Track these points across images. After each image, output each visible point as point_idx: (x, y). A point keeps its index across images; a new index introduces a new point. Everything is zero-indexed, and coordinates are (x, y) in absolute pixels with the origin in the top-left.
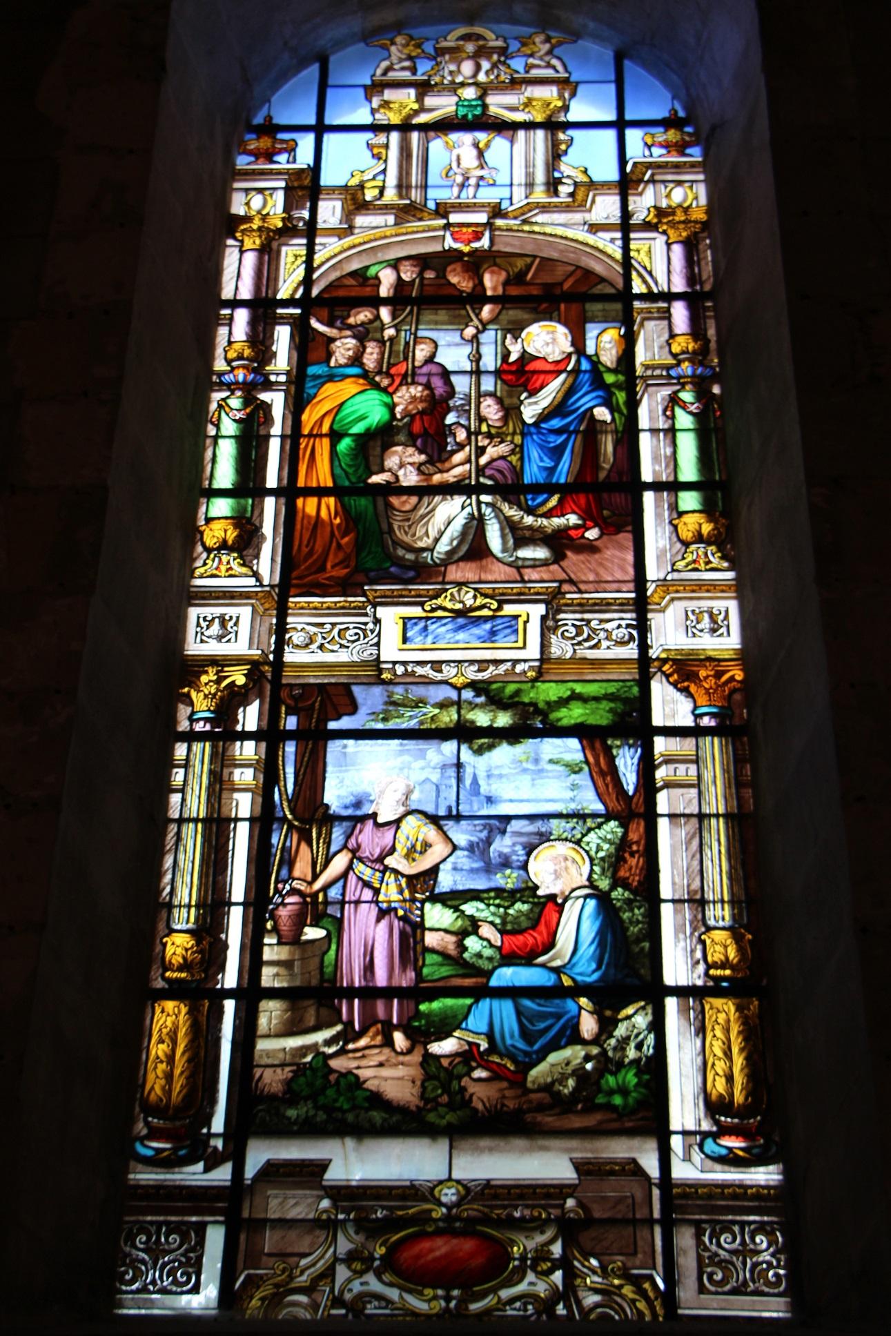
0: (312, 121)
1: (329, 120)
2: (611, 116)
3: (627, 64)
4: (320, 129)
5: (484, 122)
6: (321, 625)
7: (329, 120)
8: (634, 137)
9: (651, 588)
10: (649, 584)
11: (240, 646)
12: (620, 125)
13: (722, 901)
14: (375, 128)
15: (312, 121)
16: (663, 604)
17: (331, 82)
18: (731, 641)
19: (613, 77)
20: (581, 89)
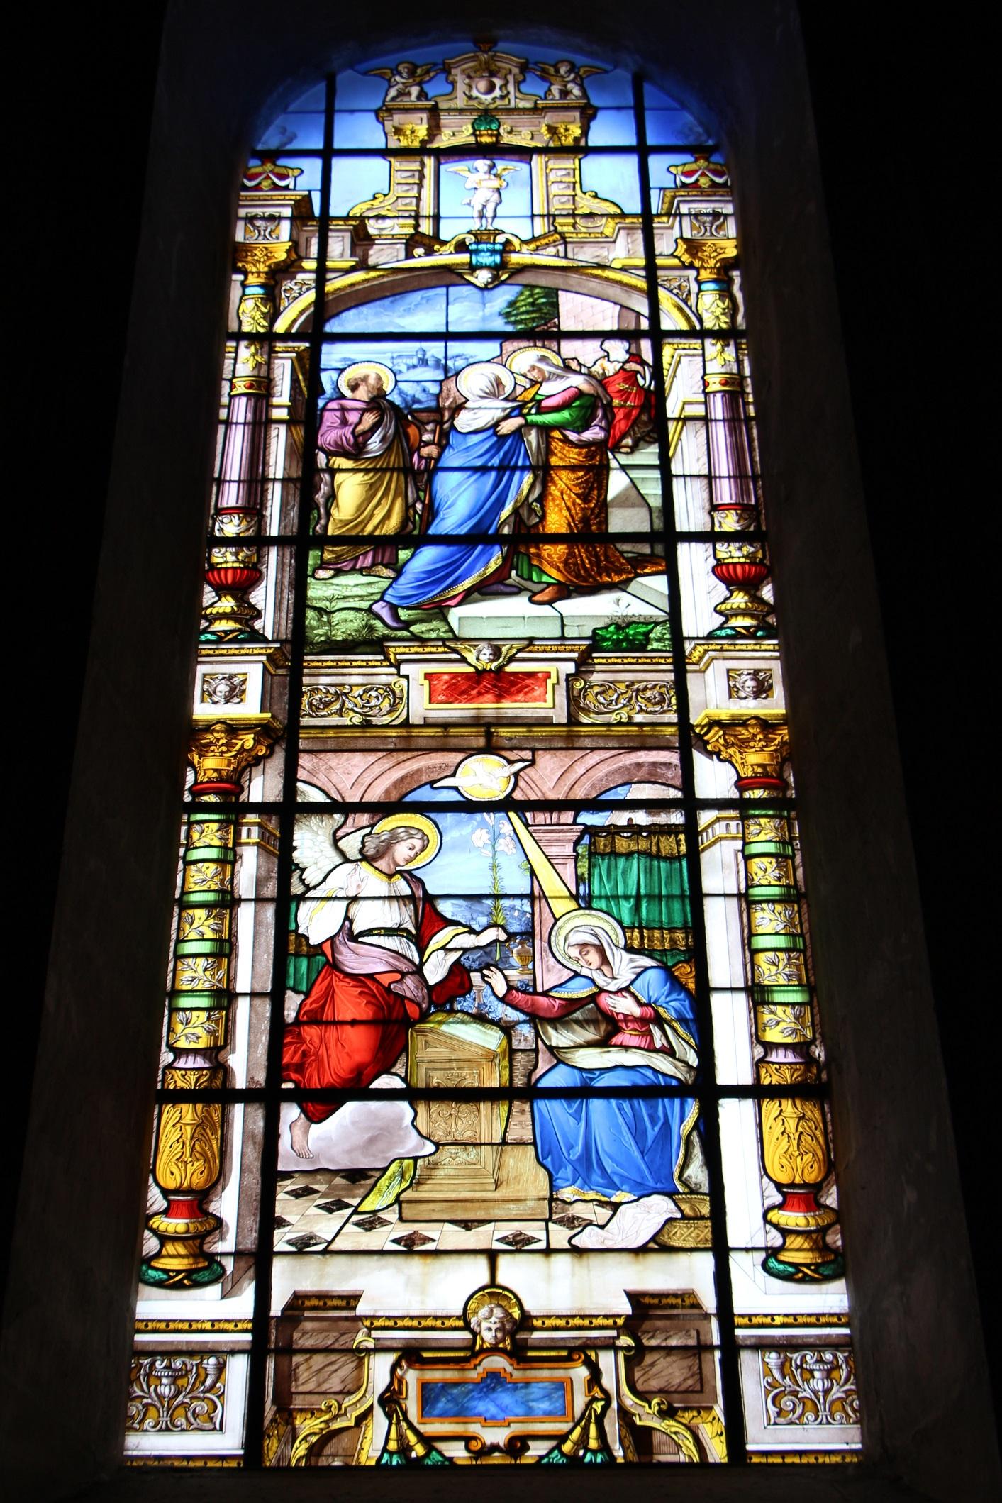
0: (319, 145)
1: (338, 144)
2: (631, 140)
3: (647, 88)
4: (328, 154)
5: (494, 151)
7: (338, 144)
8: (657, 164)
11: (250, 708)
12: (642, 151)
13: (682, 897)
14: (384, 153)
15: (319, 145)
17: (337, 107)
18: (775, 705)
19: (631, 102)
20: (600, 115)
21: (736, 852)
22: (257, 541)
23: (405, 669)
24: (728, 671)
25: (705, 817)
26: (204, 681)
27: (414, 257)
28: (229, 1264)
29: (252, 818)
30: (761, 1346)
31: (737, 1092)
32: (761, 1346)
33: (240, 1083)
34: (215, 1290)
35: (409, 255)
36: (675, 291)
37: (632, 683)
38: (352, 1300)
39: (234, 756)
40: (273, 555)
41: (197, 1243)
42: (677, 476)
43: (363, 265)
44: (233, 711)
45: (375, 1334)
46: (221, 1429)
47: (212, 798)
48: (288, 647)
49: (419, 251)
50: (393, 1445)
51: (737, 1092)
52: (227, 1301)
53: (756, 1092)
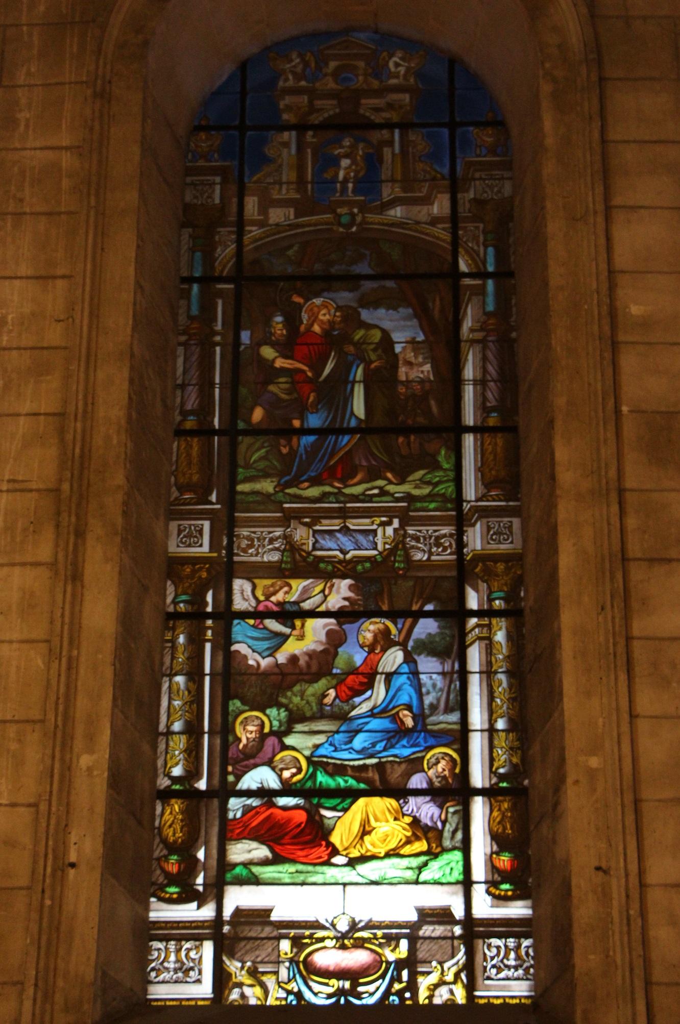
9: (466, 507)
10: (465, 504)
16: (473, 521)
28: (201, 888)
34: (195, 905)
38: (268, 912)
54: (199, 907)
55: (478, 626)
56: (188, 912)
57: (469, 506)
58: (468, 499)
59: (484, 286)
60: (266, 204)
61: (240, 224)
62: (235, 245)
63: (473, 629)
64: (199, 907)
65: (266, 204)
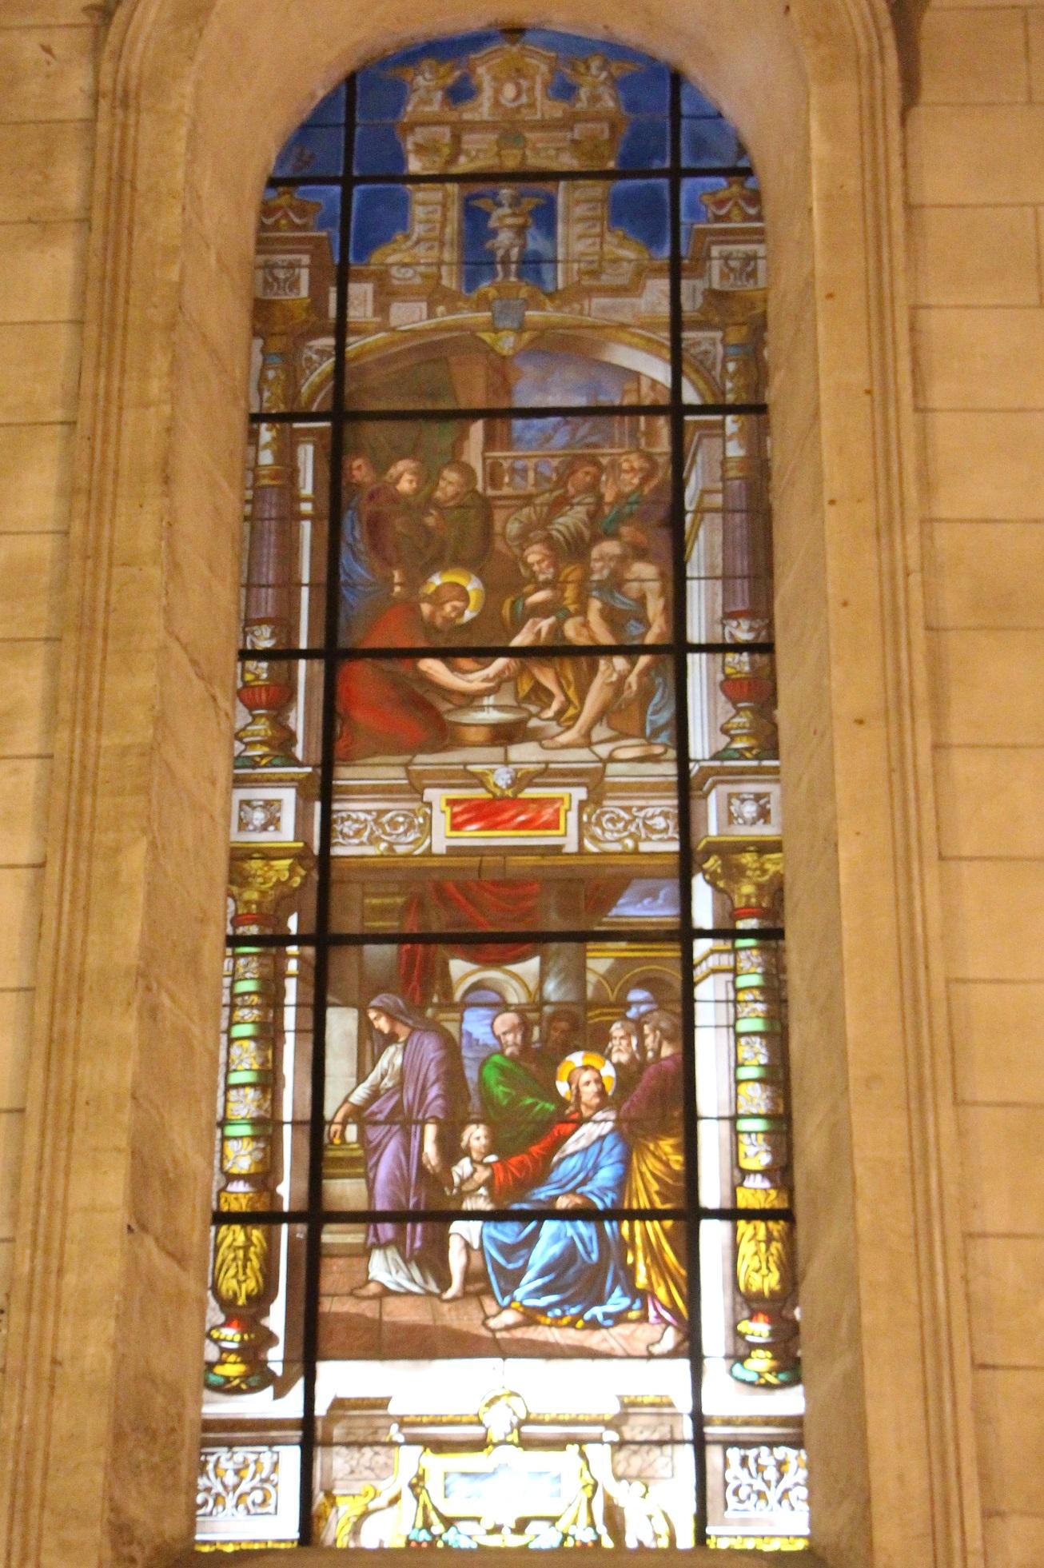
6: (368, 812)
9: (694, 768)
10: (691, 765)
21: (727, 982)
22: (284, 654)
23: (430, 794)
24: (730, 796)
25: (701, 946)
26: (241, 809)
27: (436, 317)
29: (293, 949)
30: (727, 1444)
31: (699, 648)
32: (727, 1444)
33: (286, 1208)
34: (269, 1391)
35: (431, 314)
36: (700, 357)
37: (641, 808)
38: (382, 1403)
39: (271, 888)
40: (302, 664)
41: (252, 1352)
42: (692, 578)
43: (384, 327)
44: (267, 838)
45: (406, 1430)
46: (276, 1513)
47: (254, 930)
48: (319, 771)
49: (441, 309)
50: (419, 1524)
51: (699, 648)
52: (279, 1401)
53: (732, 1214)
54: (278, 1395)
55: (713, 952)
56: (259, 1405)
57: (697, 767)
58: (699, 757)
59: (722, 425)
60: (386, 295)
61: (341, 330)
62: (333, 359)
63: (705, 958)
64: (278, 1395)
65: (386, 295)
